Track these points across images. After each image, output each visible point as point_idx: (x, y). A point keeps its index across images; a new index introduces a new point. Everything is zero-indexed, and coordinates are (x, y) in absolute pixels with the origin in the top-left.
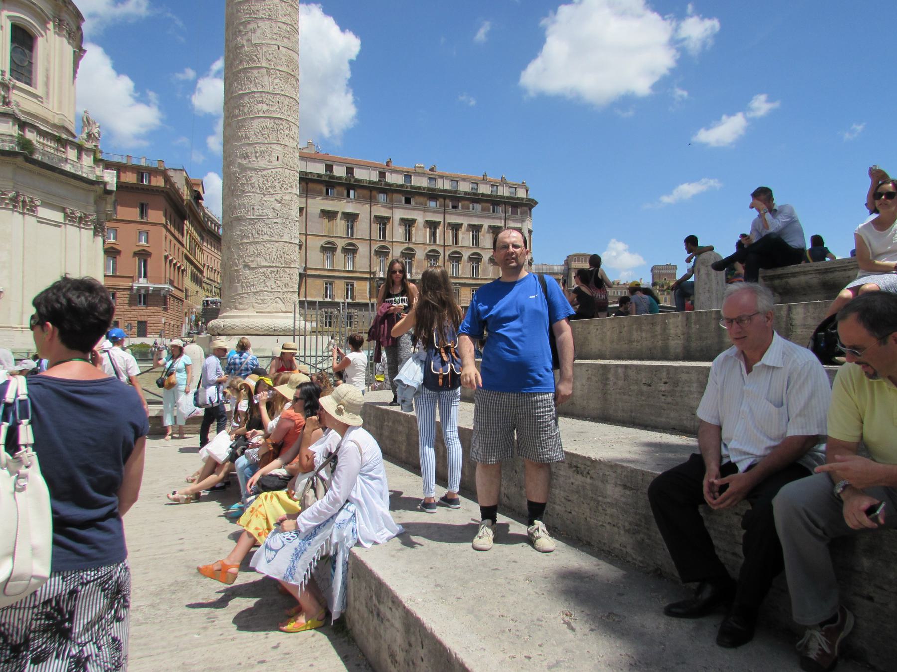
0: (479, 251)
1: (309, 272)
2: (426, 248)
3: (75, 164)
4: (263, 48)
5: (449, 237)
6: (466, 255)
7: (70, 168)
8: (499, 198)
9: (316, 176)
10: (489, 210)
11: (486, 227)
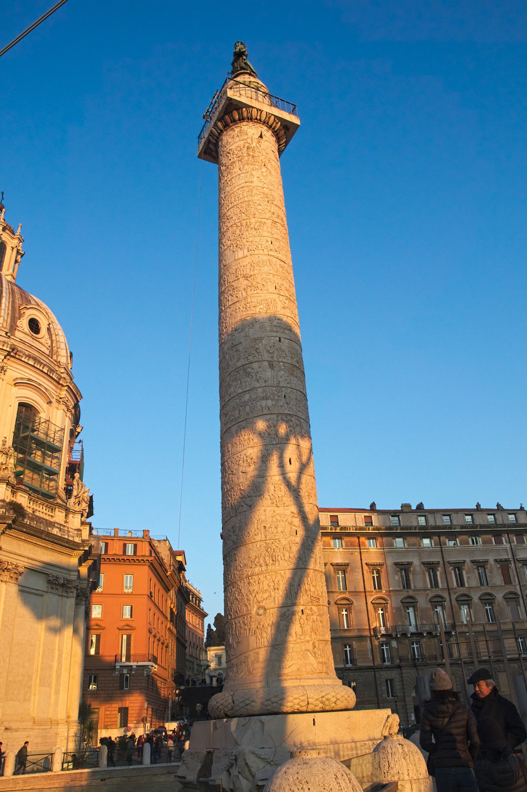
2: (428, 594)
3: (62, 527)
4: (264, 341)
5: (452, 577)
6: (475, 597)
7: (57, 532)
10: (492, 543)
11: (492, 561)
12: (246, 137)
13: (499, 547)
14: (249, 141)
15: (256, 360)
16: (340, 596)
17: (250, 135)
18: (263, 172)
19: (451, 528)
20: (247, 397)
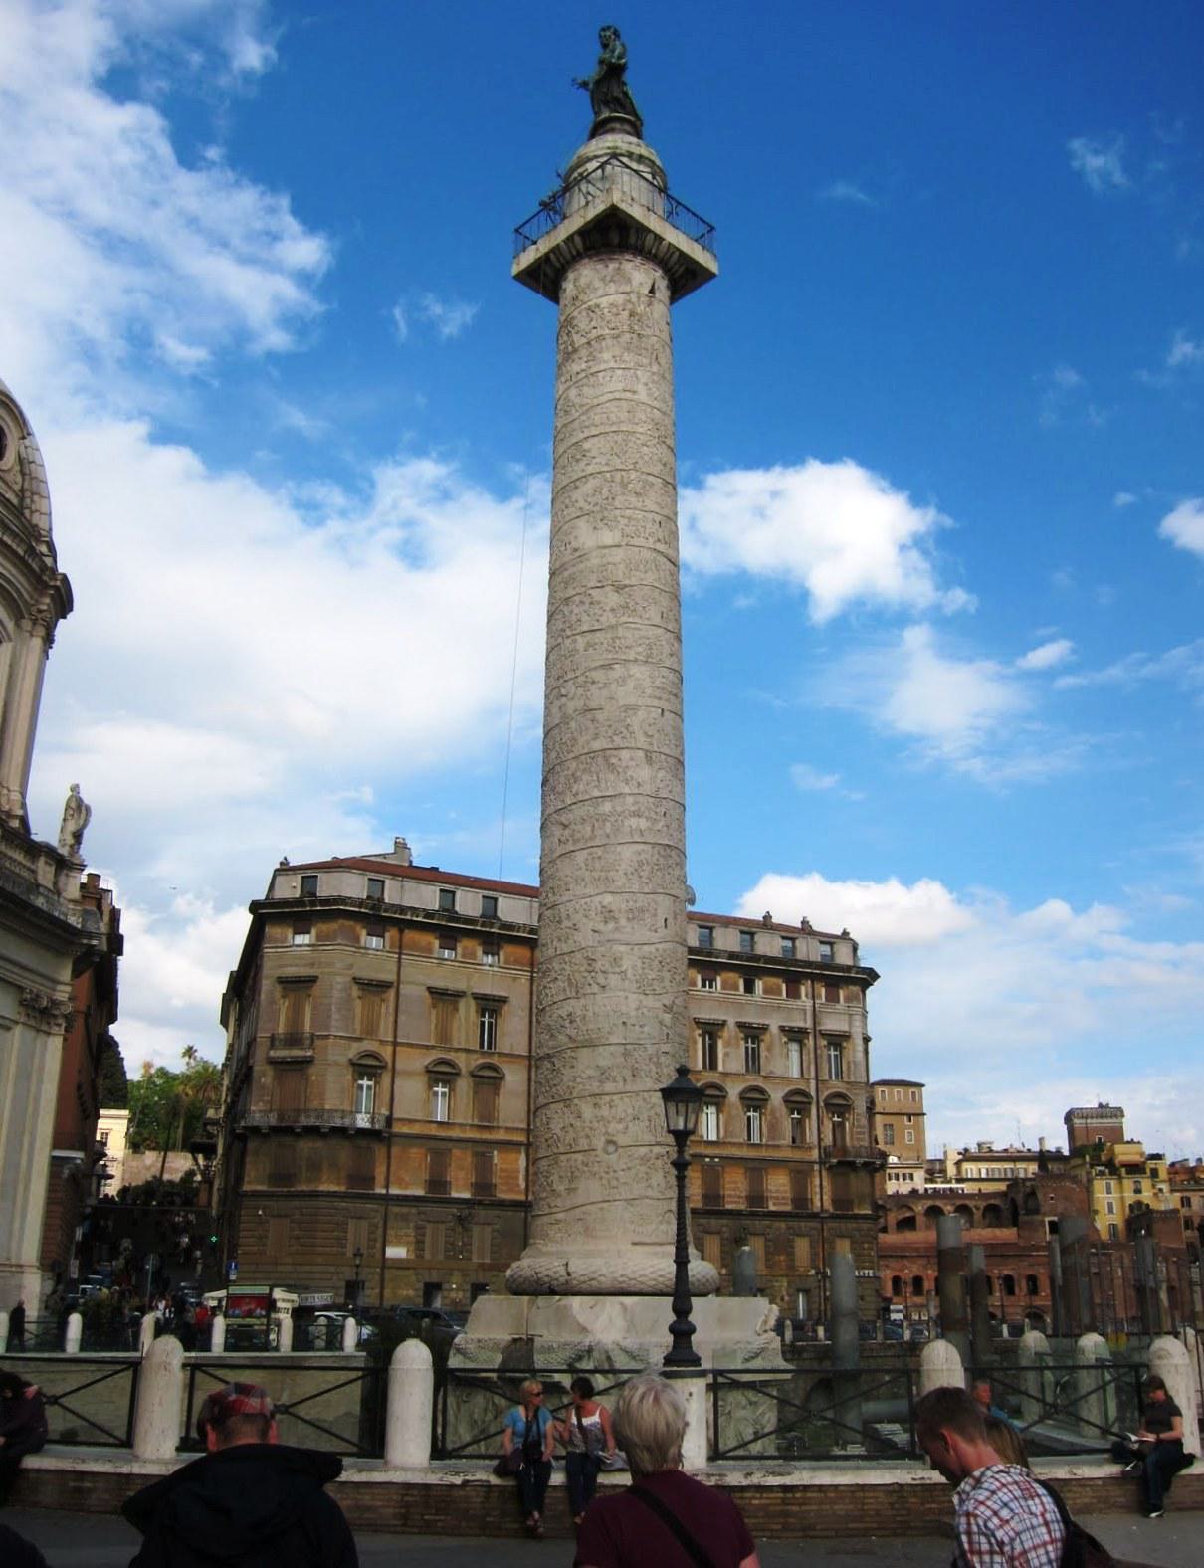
0: (760, 1083)
1: (397, 1129)
6: (734, 1091)
8: (800, 967)
9: (422, 914)
10: (780, 994)
11: (774, 1029)
12: (628, 289)
13: (792, 1003)
14: (634, 298)
15: (627, 745)
16: (481, 1061)
17: (635, 282)
18: (654, 374)
19: (710, 955)
20: (607, 807)
